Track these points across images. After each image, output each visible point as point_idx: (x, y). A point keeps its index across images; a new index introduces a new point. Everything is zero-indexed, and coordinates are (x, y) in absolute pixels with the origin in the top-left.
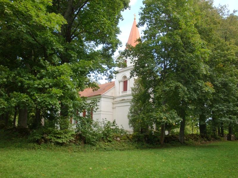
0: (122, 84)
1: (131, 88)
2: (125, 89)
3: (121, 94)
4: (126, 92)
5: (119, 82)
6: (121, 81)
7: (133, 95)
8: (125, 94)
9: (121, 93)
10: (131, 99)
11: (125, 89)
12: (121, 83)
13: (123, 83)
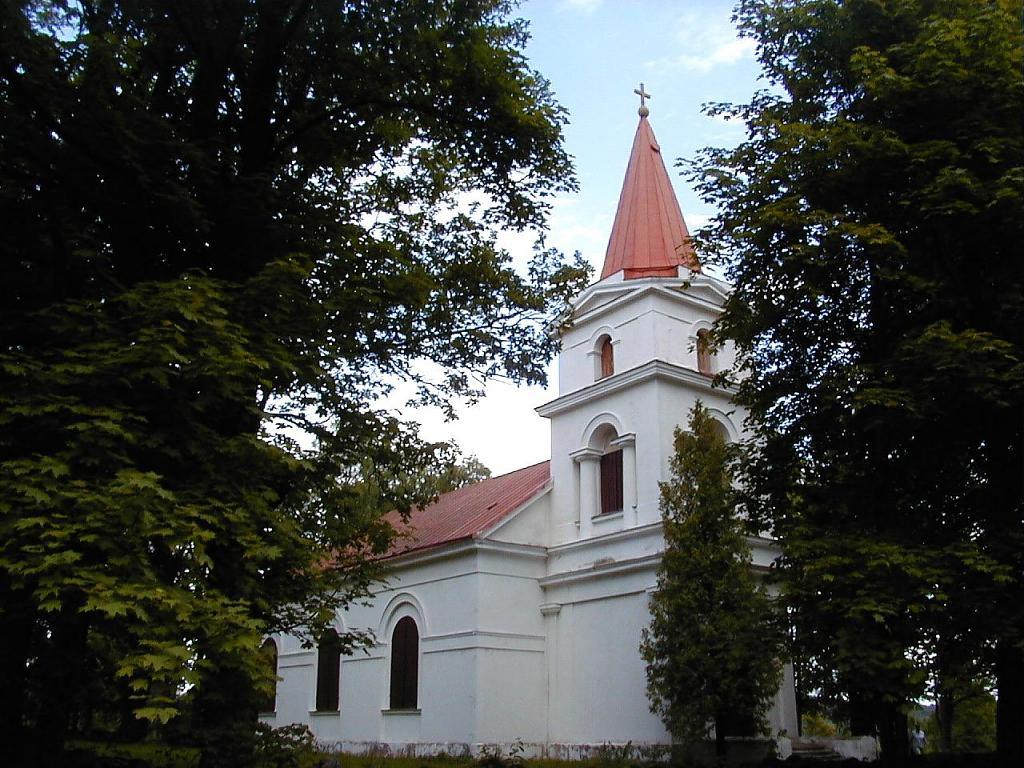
0: (590, 475)
1: (660, 485)
2: (612, 498)
3: (588, 533)
4: (618, 518)
5: (577, 464)
6: (587, 457)
7: (668, 529)
8: (611, 527)
9: (586, 522)
10: (657, 556)
11: (612, 498)
12: (584, 466)
13: (598, 467)
